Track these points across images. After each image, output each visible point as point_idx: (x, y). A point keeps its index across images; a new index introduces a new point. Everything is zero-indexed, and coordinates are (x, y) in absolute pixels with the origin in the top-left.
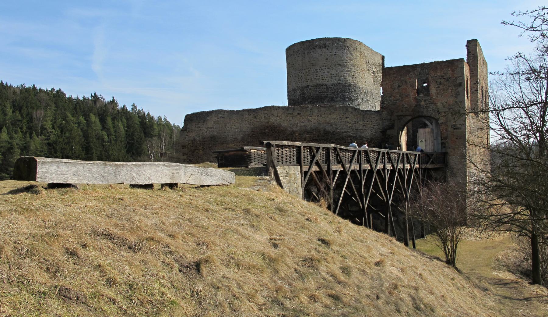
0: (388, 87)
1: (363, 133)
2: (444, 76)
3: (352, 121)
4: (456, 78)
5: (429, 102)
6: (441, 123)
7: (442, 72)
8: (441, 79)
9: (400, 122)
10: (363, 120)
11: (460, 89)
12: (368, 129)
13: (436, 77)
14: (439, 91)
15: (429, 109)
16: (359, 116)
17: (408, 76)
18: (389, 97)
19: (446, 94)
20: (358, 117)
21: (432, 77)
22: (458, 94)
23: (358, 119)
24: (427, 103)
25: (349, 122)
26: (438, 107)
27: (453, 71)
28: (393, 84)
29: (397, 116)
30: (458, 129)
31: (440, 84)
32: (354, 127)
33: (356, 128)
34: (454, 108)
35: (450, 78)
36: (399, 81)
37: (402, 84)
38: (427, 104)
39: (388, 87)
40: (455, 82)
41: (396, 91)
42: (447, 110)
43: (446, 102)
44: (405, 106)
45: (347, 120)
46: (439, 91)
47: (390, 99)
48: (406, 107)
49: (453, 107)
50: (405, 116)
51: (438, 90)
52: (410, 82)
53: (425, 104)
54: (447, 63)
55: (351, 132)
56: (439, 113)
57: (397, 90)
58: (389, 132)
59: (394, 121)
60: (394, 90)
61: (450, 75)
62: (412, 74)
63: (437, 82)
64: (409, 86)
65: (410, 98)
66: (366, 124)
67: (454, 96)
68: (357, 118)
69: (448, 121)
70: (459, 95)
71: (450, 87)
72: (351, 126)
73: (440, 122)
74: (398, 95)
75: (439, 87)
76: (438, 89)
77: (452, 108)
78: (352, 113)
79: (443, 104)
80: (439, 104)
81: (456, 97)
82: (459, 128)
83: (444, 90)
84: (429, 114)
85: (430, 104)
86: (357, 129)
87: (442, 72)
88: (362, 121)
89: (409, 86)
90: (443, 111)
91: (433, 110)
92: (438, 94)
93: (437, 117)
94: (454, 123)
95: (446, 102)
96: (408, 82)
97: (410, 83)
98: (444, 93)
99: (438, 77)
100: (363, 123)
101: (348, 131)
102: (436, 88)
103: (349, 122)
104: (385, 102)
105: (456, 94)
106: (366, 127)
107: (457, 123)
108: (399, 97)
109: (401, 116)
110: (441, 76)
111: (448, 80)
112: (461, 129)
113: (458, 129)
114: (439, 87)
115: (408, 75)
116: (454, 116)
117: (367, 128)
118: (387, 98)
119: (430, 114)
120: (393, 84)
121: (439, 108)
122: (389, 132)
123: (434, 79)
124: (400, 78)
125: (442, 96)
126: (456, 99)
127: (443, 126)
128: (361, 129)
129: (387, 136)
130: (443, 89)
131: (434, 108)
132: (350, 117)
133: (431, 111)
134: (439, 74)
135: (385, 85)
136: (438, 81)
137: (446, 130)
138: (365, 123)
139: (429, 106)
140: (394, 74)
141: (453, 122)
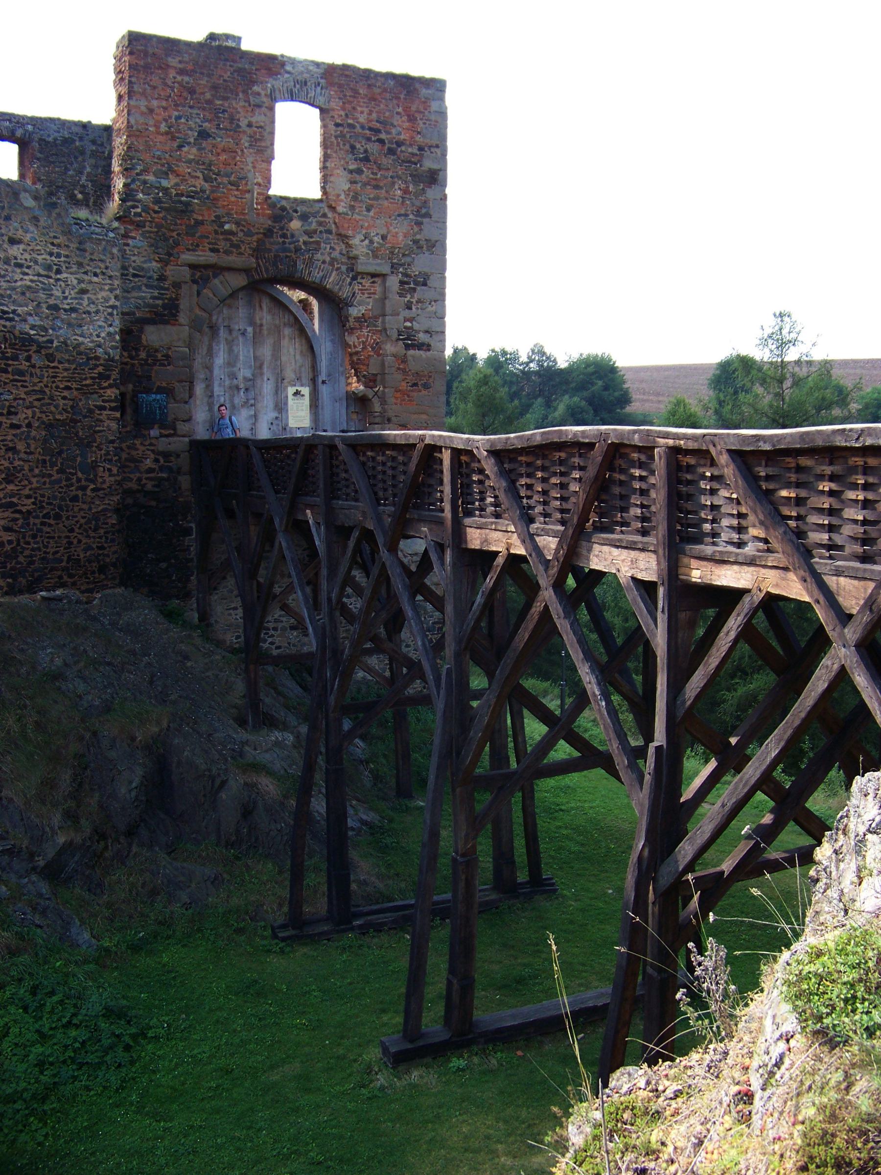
0: (157, 127)
1: (78, 332)
2: (378, 131)
3: (36, 262)
4: (421, 149)
5: (320, 224)
6: (357, 319)
7: (374, 116)
8: (369, 139)
9: (199, 294)
10: (80, 265)
11: (431, 193)
12: (97, 312)
13: (351, 126)
14: (359, 186)
15: (318, 256)
16: (62, 240)
17: (241, 95)
18: (158, 174)
19: (386, 203)
20: (59, 246)
21: (337, 125)
22: (424, 211)
23: (59, 255)
24: (314, 226)
25: (20, 266)
26: (355, 252)
27: (412, 119)
28: (179, 117)
29: (193, 267)
30: (422, 346)
31: (366, 159)
32: (42, 296)
33: (52, 302)
34: (409, 265)
35: (399, 144)
36: (204, 109)
37: (218, 128)
38: (309, 233)
39: (157, 127)
40: (416, 164)
41: (191, 152)
42: (386, 269)
43: (384, 237)
44: (227, 227)
45: (15, 251)
46: (359, 186)
47: (165, 183)
48: (231, 233)
49: (408, 259)
50: (218, 270)
51: (355, 182)
52: (250, 125)
53: (306, 233)
54: (392, 83)
55: (31, 320)
56: (354, 278)
57: (194, 150)
58: (153, 336)
59: (177, 285)
60: (180, 147)
61: (399, 134)
62: (259, 94)
63: (353, 147)
64: (245, 141)
65: (247, 196)
66: (90, 288)
67: (411, 216)
68: (56, 250)
69: (388, 310)
70: (428, 215)
71: (400, 178)
72: (29, 287)
73: (354, 312)
74: (200, 175)
75: (359, 171)
76: (357, 177)
77: (402, 265)
78: (36, 219)
79: (371, 242)
80: (355, 241)
81: (418, 224)
82: (423, 344)
83: (377, 187)
84: (316, 276)
85: (325, 235)
86: (55, 308)
87: (374, 116)
88: (74, 268)
89: (245, 141)
90: (371, 269)
91: (333, 260)
92: (355, 198)
93: (345, 293)
94: (408, 324)
95: (384, 237)
96: (243, 123)
97: (249, 131)
98: (377, 198)
99: (358, 129)
100: (80, 281)
101: (20, 310)
102: (351, 172)
103: (20, 266)
104: (141, 196)
105: (418, 213)
106: (91, 302)
107: (416, 326)
108: (200, 183)
109: (207, 267)
110: (370, 129)
111: (391, 152)
112: (427, 347)
113: (422, 346)
114: (359, 171)
115: (245, 92)
116: (409, 296)
117: (92, 308)
118: (151, 178)
119: (321, 274)
120: (179, 117)
121: (355, 258)
122: (153, 336)
123: (342, 136)
124: (208, 96)
125: (368, 210)
126: (416, 229)
127: (365, 331)
128: (73, 310)
129: (143, 355)
130: (374, 183)
131: (335, 254)
132: (29, 236)
133: (324, 262)
134: (362, 119)
135: (142, 114)
136: (358, 146)
137: (377, 348)
138: (86, 277)
139: (318, 243)
140: (181, 72)
141: (405, 321)
